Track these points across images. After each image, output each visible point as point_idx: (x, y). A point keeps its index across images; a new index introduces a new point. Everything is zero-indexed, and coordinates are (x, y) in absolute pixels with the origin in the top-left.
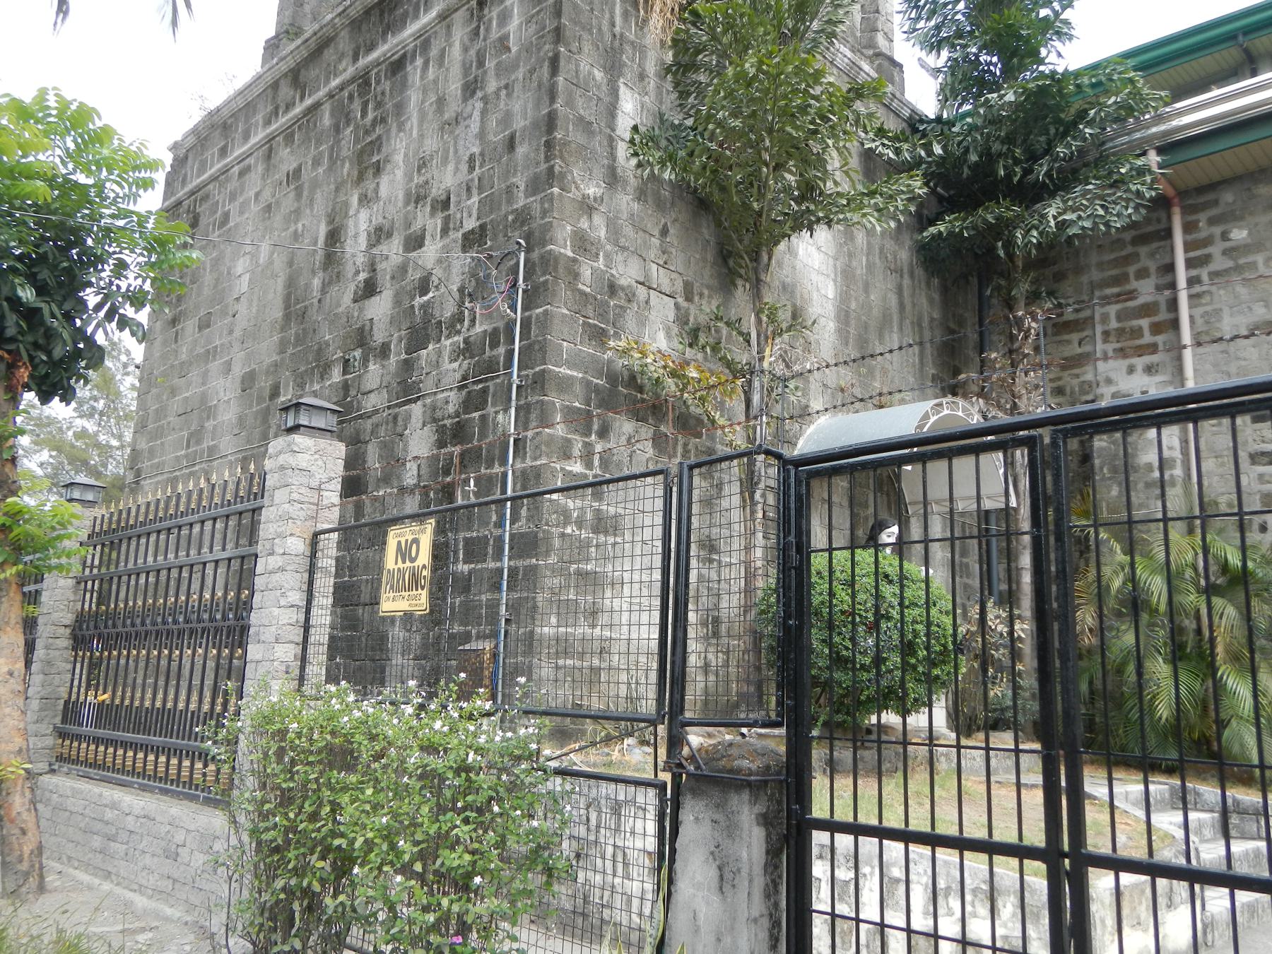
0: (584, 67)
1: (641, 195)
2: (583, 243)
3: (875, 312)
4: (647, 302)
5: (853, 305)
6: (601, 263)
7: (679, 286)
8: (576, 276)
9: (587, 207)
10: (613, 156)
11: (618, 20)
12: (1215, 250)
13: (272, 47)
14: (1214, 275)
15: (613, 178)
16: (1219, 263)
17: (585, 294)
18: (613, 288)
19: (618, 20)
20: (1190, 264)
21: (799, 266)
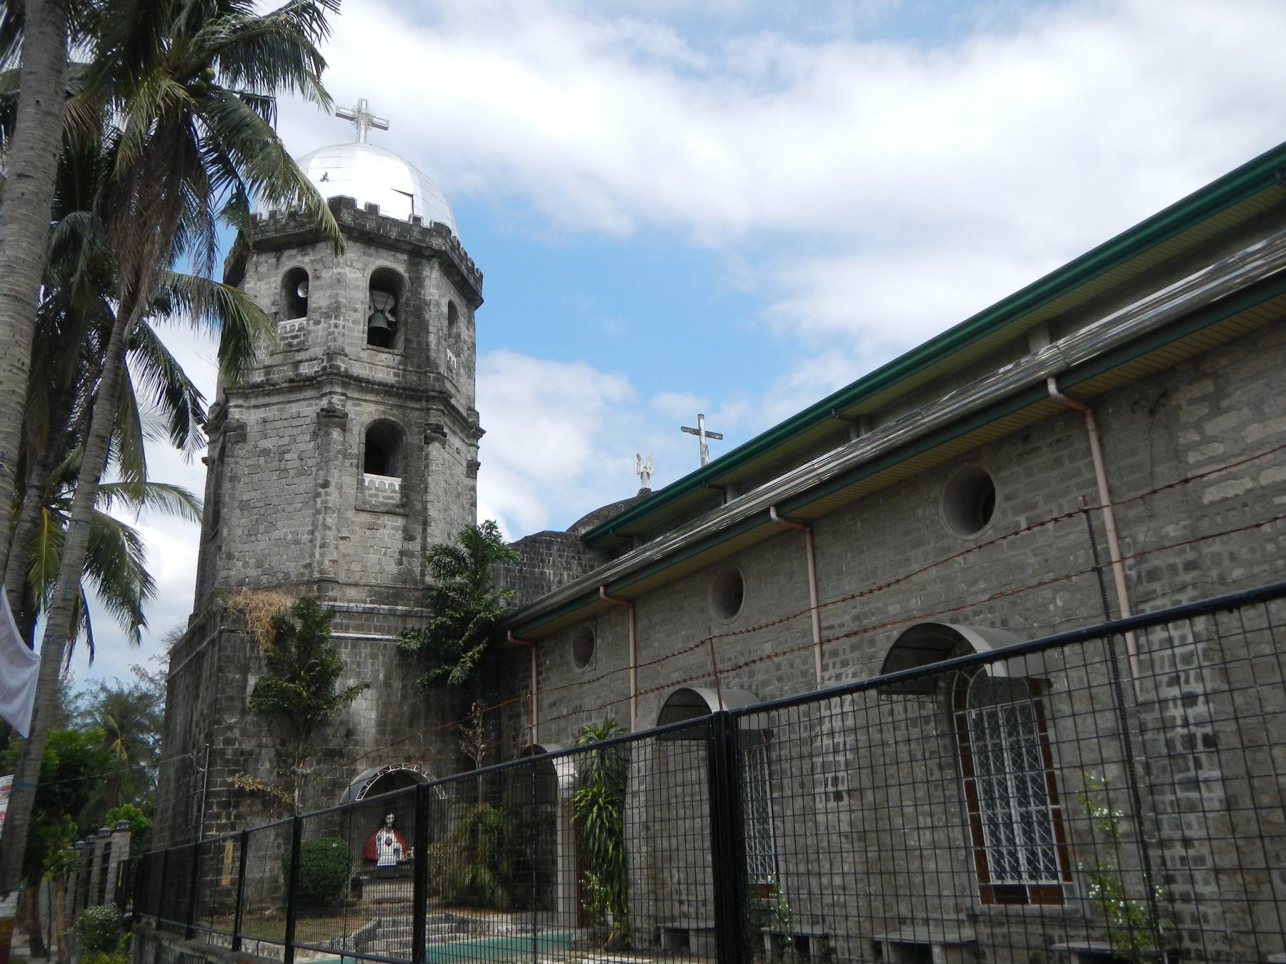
0: (230, 676)
1: (261, 712)
2: (228, 742)
3: (407, 714)
4: (260, 753)
5: (390, 716)
6: (237, 746)
7: (278, 741)
8: (225, 754)
9: (230, 728)
10: (244, 704)
11: (248, 652)
12: (543, 669)
13: (192, 618)
14: (544, 680)
15: (244, 712)
16: (544, 675)
17: (228, 760)
18: (242, 753)
19: (248, 652)
20: (539, 674)
21: (352, 710)
